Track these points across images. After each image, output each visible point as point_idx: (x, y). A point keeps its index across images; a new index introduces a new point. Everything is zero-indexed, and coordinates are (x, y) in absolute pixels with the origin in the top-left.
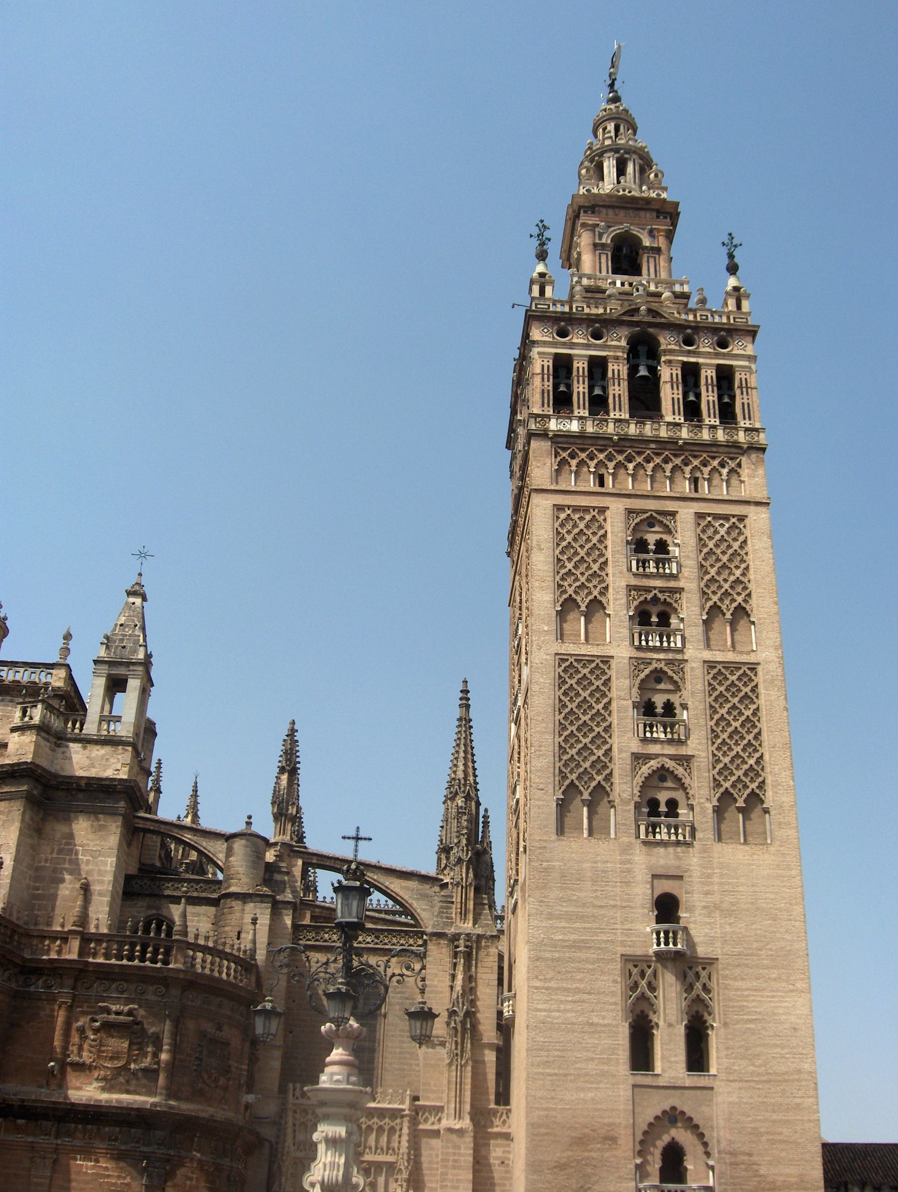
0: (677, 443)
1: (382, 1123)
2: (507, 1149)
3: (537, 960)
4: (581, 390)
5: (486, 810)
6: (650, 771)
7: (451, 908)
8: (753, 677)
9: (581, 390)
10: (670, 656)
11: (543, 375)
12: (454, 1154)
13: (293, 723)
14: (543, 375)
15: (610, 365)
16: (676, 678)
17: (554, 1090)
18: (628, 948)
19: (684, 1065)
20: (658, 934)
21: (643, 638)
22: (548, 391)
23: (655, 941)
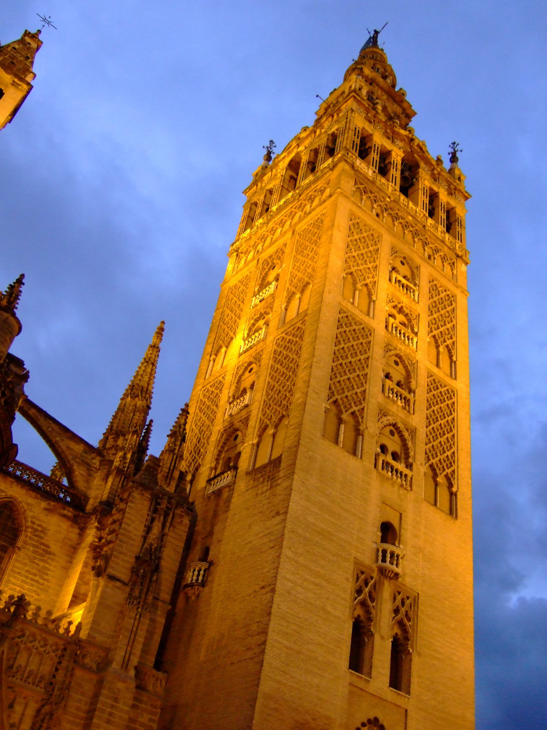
0: (424, 226)
1: (43, 649)
2: (153, 717)
3: (293, 532)
4: (375, 156)
5: (151, 421)
6: (388, 423)
7: (157, 471)
8: (452, 397)
9: (375, 156)
10: (408, 351)
11: (355, 133)
12: (112, 707)
13: (23, 276)
14: (355, 133)
15: (393, 157)
16: (409, 367)
17: (287, 664)
18: (359, 555)
19: (388, 680)
20: (384, 552)
21: (394, 329)
22: (357, 144)
23: (380, 558)
